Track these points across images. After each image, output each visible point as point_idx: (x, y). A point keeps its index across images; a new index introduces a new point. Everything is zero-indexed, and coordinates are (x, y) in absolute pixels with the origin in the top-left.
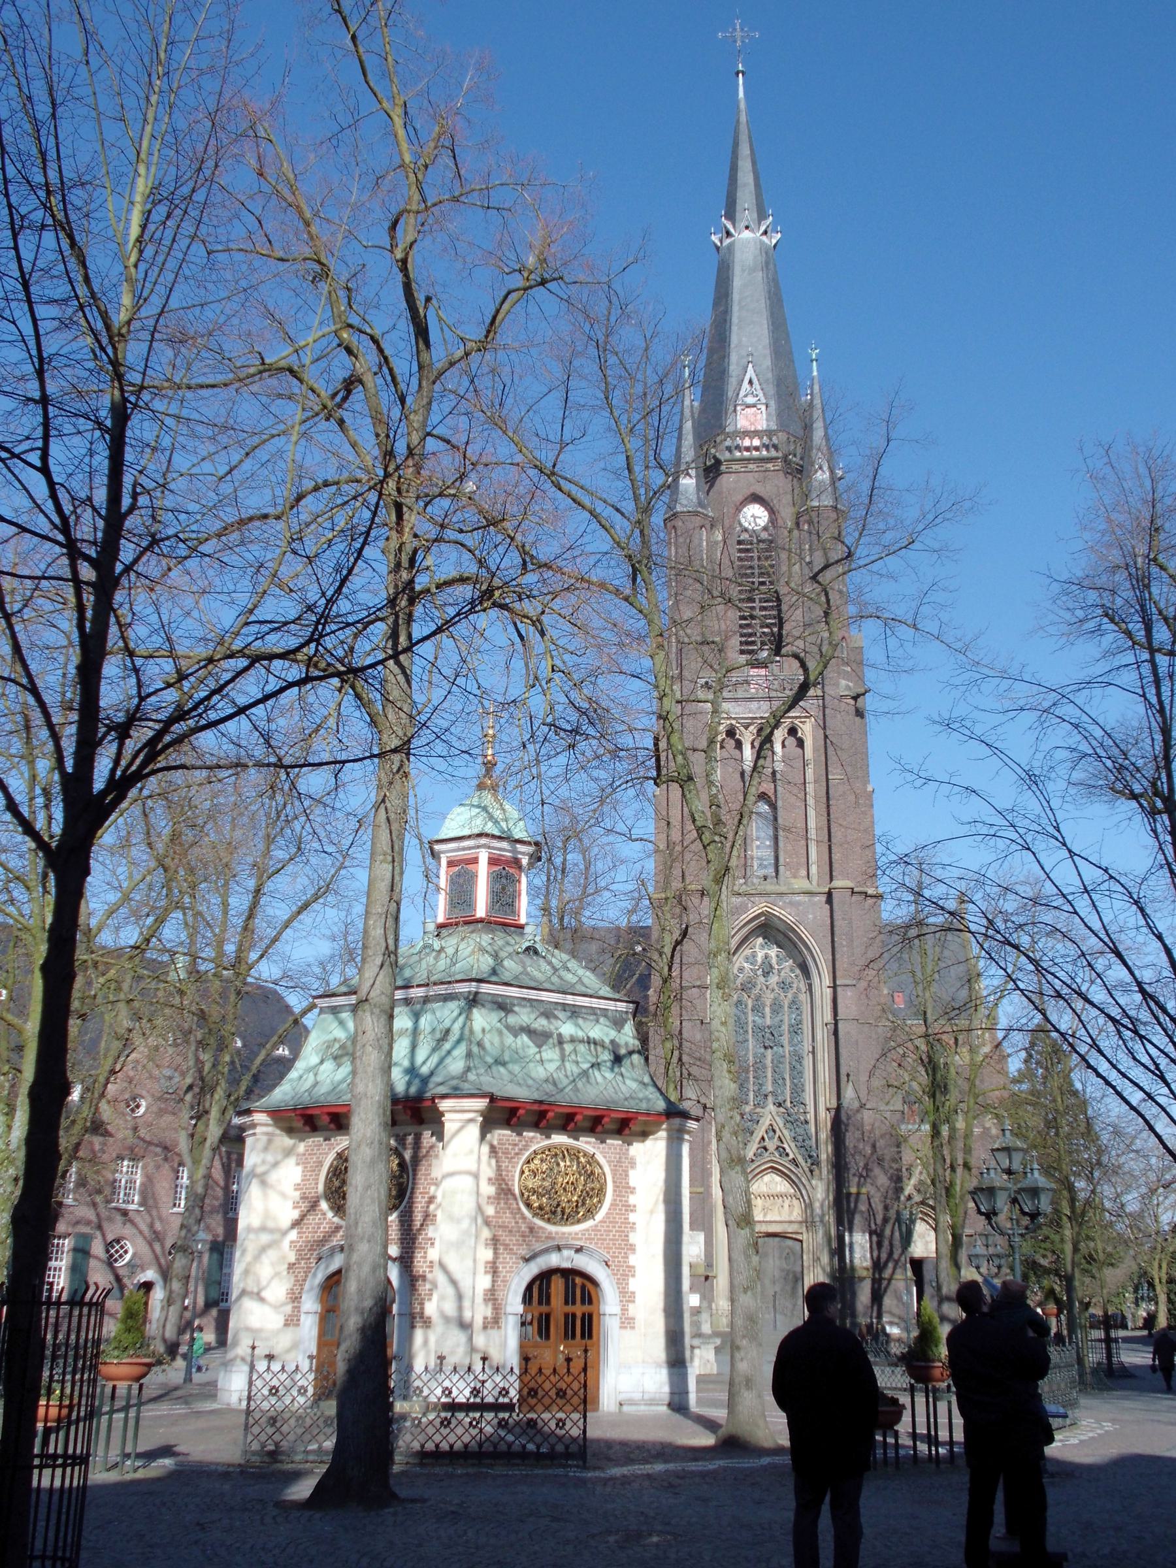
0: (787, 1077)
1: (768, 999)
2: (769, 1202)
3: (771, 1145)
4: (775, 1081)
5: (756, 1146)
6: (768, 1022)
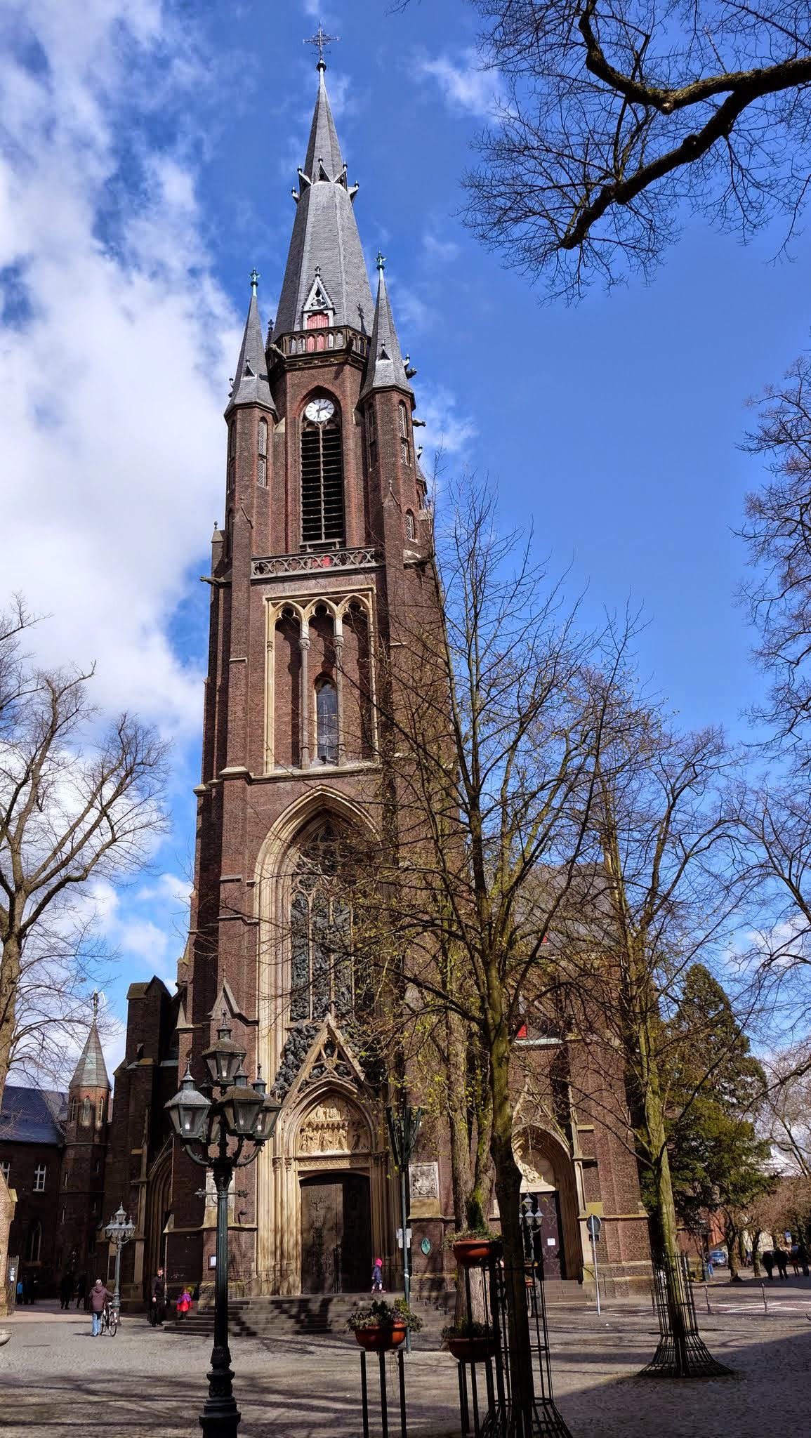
2: (328, 1135)
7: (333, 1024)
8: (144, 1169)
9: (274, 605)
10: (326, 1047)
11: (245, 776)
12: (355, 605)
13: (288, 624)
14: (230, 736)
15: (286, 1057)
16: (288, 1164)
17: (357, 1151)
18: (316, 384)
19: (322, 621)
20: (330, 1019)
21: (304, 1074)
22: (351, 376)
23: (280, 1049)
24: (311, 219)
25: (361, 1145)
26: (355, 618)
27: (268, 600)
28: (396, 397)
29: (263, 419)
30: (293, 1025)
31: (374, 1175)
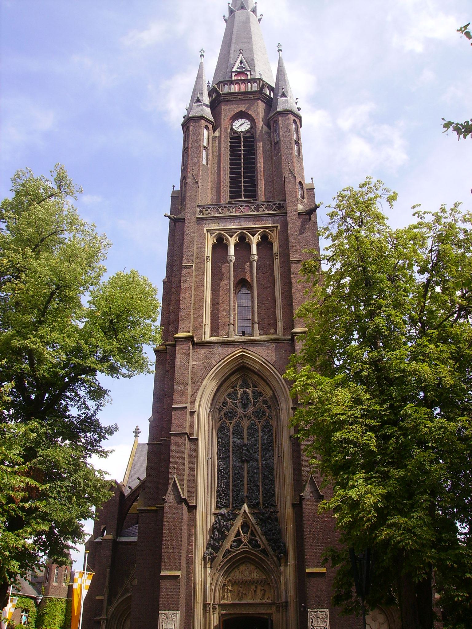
0: (260, 484)
1: (245, 424)
3: (244, 538)
4: (250, 489)
5: (233, 538)
6: (245, 441)
7: (247, 510)
8: (105, 610)
9: (211, 234)
10: (242, 527)
11: (190, 339)
12: (264, 237)
13: (220, 245)
14: (180, 313)
15: (214, 533)
16: (214, 608)
17: (264, 601)
18: (240, 109)
19: (243, 244)
20: (245, 506)
21: (227, 545)
22: (261, 106)
23: (209, 527)
24: (236, 28)
25: (266, 597)
26: (265, 243)
27: (208, 231)
28: (292, 118)
29: (206, 127)
30: (217, 512)
31: (276, 617)
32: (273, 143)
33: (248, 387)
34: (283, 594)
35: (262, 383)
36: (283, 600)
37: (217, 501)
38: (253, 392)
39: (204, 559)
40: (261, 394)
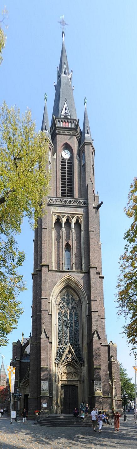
10: (68, 352)
15: (57, 354)
17: (75, 380)
21: (63, 359)
25: (76, 378)
31: (79, 386)
32: (81, 166)
33: (69, 296)
34: (83, 376)
35: (75, 294)
36: (83, 379)
37: (58, 342)
38: (71, 299)
39: (55, 363)
40: (74, 300)
